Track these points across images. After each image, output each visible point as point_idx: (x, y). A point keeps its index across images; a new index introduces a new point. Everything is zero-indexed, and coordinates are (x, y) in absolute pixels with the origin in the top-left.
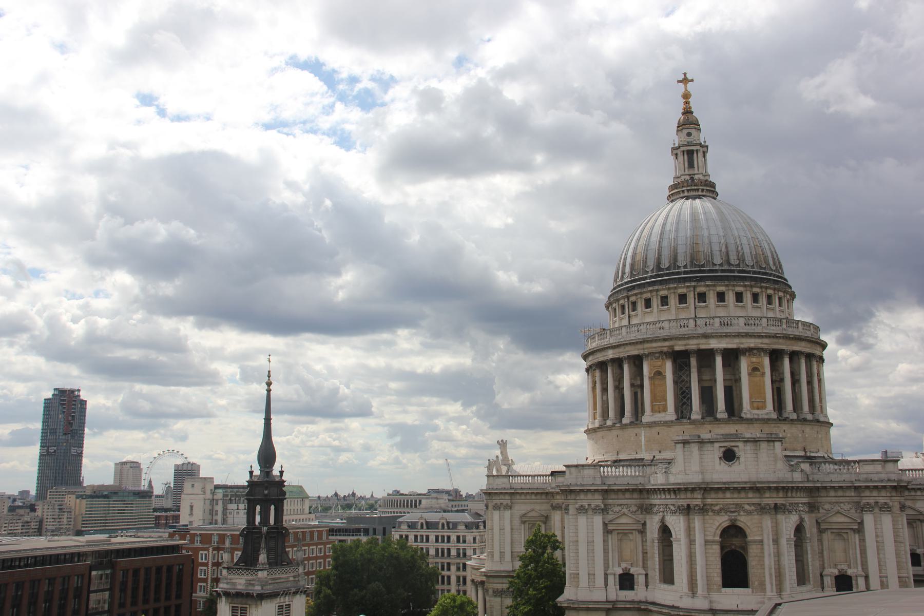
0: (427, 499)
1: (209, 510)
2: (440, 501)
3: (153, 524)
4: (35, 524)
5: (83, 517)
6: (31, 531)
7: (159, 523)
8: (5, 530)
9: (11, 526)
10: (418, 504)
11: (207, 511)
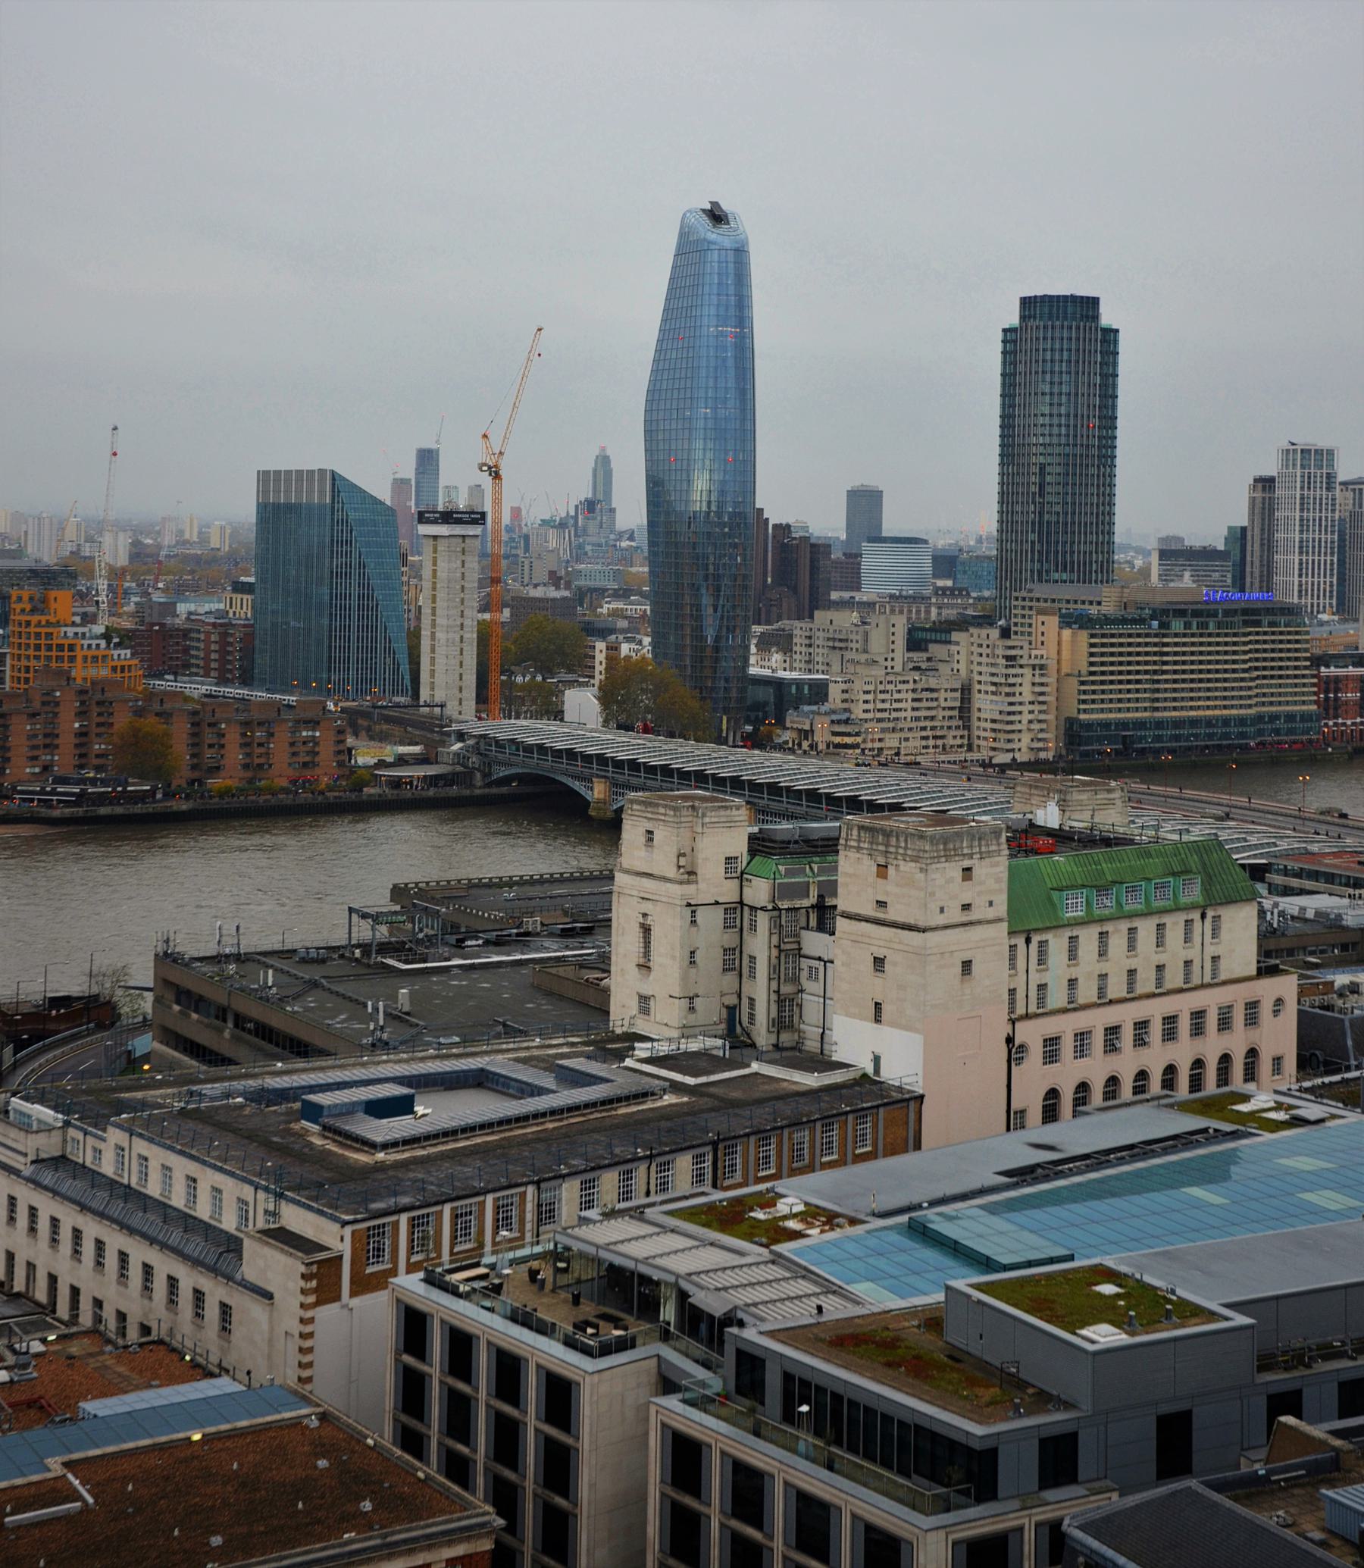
1: (718, 954)
3: (1311, 702)
4: (949, 695)
5: (1083, 683)
6: (941, 714)
7: (1336, 699)
8: (866, 711)
9: (883, 701)
11: (710, 959)
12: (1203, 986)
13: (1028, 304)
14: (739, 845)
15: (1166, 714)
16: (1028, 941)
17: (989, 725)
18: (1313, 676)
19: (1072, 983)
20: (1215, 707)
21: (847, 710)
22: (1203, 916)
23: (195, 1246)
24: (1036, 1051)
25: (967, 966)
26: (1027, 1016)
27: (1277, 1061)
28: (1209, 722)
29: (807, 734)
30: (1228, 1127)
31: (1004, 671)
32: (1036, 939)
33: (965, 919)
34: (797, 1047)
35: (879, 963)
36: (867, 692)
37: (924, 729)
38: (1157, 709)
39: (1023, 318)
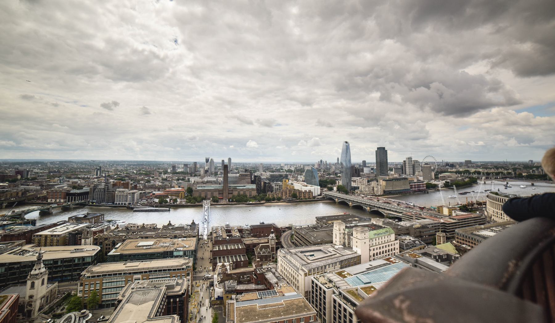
11: (342, 238)
14: (344, 227)
23: (295, 268)
24: (372, 250)
25: (365, 243)
26: (371, 247)
27: (397, 249)
28: (399, 190)
29: (357, 192)
30: (389, 263)
34: (350, 247)
35: (357, 242)
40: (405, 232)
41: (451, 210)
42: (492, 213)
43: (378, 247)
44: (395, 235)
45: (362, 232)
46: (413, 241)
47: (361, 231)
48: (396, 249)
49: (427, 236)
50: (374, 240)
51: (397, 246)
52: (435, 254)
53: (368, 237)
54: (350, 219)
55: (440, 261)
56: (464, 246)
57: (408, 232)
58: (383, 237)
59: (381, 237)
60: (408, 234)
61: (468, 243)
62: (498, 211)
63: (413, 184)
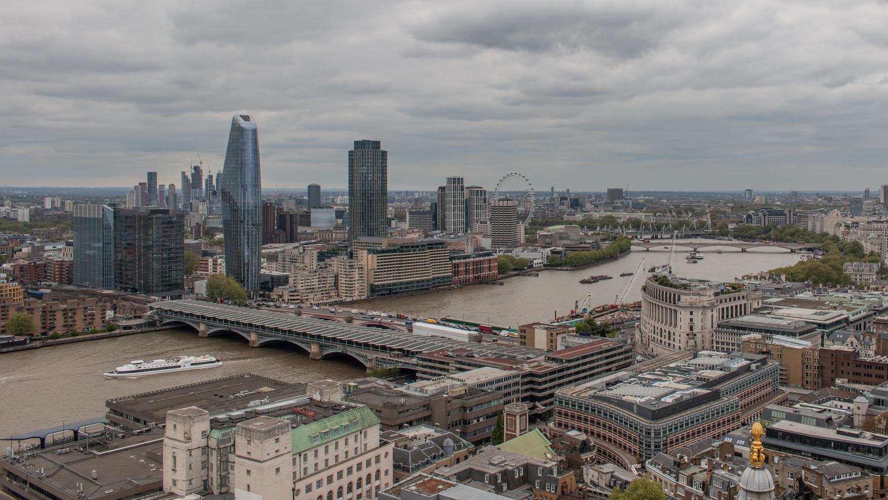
0: (686, 294)
2: (702, 298)
3: (450, 272)
5: (375, 272)
6: (328, 285)
9: (308, 282)
10: (676, 300)
12: (362, 454)
13: (357, 143)
15: (403, 280)
16: (300, 455)
17: (344, 288)
18: (450, 264)
19: (316, 465)
20: (419, 277)
21: (295, 287)
22: (361, 433)
27: (386, 473)
28: (418, 282)
31: (349, 270)
32: (303, 454)
33: (277, 455)
36: (302, 280)
37: (322, 291)
38: (400, 279)
39: (355, 148)
40: (420, 416)
41: (554, 335)
42: (650, 334)
43: (324, 475)
44: (384, 426)
45: (269, 433)
46: (435, 440)
47: (265, 433)
48: (382, 474)
49: (481, 420)
50: (311, 455)
51: (387, 464)
52: (493, 470)
53: (289, 449)
54: (242, 393)
55: (505, 488)
56: (573, 433)
57: (427, 413)
58: (342, 442)
59: (334, 443)
60: (427, 420)
61: (583, 425)
62: (664, 327)
63: (462, 260)
